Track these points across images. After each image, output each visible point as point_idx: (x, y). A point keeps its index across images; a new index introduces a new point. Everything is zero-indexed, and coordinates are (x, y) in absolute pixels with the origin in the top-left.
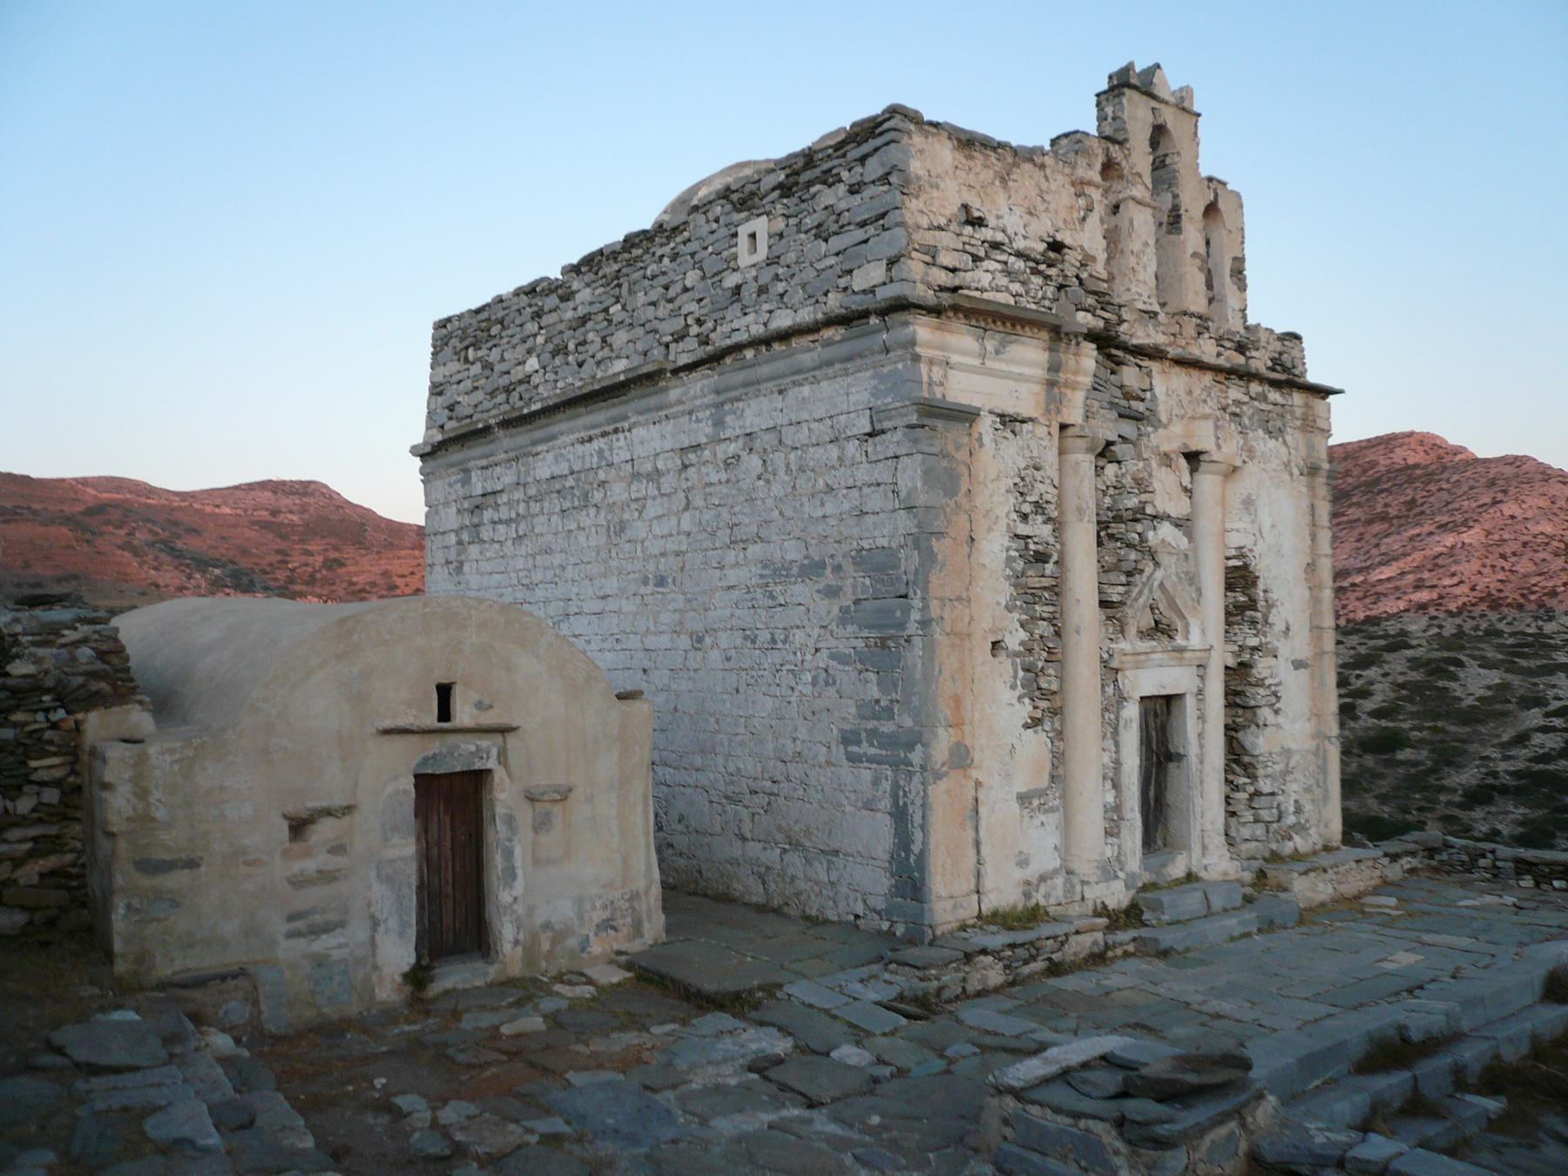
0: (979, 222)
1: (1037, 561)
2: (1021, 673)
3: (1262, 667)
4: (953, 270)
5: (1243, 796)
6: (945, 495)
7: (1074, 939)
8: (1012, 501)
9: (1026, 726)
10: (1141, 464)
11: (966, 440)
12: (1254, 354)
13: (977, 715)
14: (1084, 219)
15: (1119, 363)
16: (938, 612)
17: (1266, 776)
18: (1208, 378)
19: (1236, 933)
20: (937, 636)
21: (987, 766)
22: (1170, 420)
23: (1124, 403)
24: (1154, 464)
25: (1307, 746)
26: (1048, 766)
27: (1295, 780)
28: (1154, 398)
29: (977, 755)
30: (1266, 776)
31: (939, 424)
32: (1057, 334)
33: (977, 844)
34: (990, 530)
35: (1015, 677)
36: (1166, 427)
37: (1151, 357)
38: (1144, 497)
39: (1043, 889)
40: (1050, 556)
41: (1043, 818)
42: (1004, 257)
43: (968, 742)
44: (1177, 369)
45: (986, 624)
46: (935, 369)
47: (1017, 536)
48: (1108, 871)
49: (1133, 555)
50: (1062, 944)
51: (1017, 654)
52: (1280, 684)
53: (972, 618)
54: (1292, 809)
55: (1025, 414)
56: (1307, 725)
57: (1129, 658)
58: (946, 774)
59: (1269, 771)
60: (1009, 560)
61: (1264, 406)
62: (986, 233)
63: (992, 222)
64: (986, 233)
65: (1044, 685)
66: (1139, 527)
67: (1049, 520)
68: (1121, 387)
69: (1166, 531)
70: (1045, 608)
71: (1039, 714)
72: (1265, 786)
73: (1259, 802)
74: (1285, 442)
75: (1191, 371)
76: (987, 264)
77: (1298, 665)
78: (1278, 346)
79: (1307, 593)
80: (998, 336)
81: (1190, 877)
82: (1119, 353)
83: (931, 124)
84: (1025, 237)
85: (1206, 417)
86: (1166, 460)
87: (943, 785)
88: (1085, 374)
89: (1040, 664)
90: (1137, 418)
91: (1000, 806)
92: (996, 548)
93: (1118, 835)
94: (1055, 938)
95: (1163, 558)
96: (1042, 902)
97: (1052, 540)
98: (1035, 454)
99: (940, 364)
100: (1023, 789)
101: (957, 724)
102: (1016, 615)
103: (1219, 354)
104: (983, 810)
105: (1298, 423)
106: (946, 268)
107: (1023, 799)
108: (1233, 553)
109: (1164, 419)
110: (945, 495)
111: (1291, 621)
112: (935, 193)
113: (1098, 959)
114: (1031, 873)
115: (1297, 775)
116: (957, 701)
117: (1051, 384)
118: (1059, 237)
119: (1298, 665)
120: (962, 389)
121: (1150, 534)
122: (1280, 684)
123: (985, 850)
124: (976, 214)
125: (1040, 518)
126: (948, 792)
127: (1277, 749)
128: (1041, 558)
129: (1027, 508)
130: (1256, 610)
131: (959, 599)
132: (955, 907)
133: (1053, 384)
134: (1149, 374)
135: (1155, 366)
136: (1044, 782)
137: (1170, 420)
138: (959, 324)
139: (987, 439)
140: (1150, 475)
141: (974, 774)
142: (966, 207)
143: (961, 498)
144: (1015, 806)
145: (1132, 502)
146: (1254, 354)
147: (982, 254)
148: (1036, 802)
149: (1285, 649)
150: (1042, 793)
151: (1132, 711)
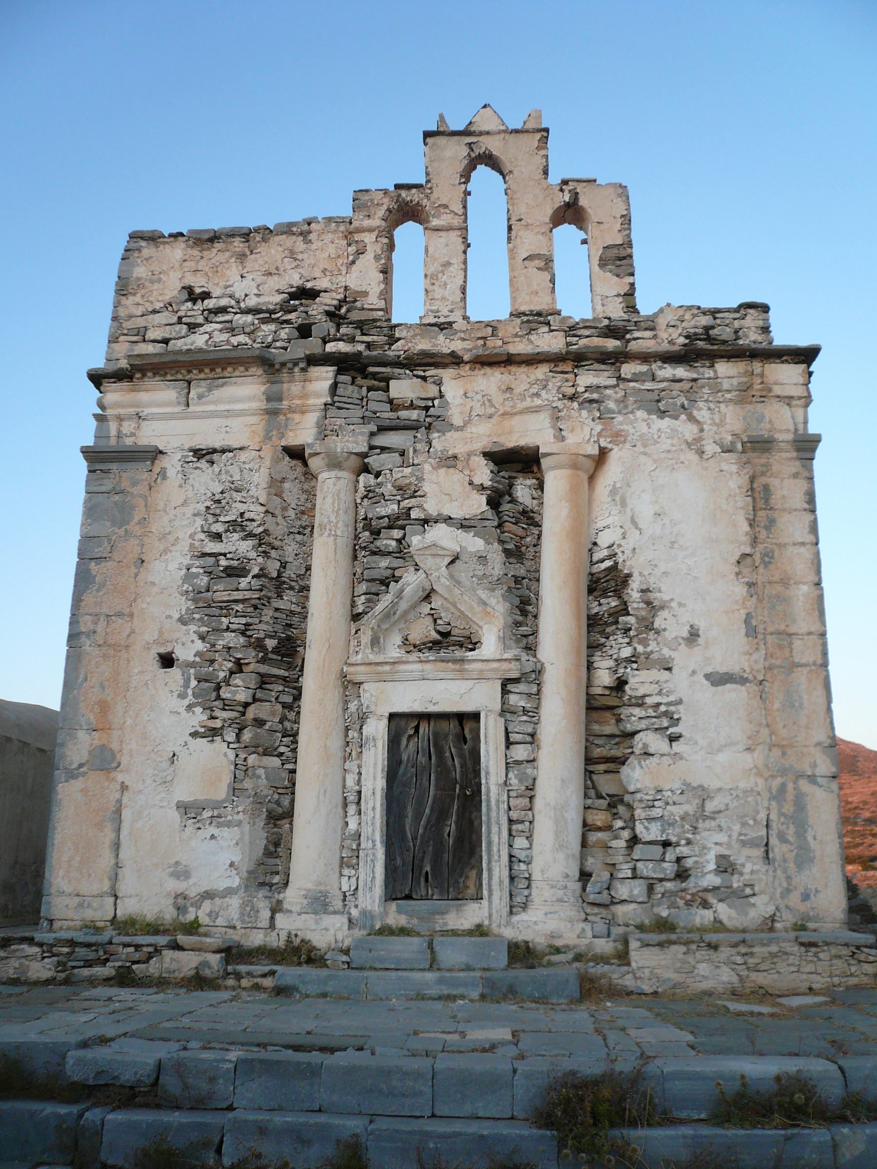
0: (206, 295)
1: (229, 576)
2: (193, 683)
3: (640, 682)
4: (166, 341)
5: (621, 844)
6: (113, 525)
7: (168, 954)
8: (199, 522)
9: (195, 735)
10: (407, 471)
11: (145, 475)
12: (637, 334)
13: (129, 722)
14: (353, 262)
15: (387, 380)
16: (91, 627)
17: (650, 819)
18: (541, 372)
19: (434, 992)
20: (87, 648)
21: (137, 770)
22: (467, 423)
23: (392, 415)
24: (427, 467)
25: (743, 785)
26: (227, 778)
27: (720, 828)
28: (445, 405)
29: (125, 760)
30: (650, 819)
31: (114, 466)
32: (269, 365)
33: (117, 846)
34: (166, 551)
35: (186, 685)
36: (460, 429)
37: (436, 365)
38: (406, 503)
39: (207, 906)
40: (249, 571)
41: (215, 831)
42: (227, 317)
43: (115, 746)
44: (488, 370)
45: (150, 635)
46: (125, 424)
47: (204, 555)
48: (319, 903)
49: (384, 562)
50: (150, 957)
51: (192, 665)
52: (680, 702)
53: (133, 632)
54: (712, 866)
55: (236, 445)
56: (748, 760)
57: (362, 669)
58: (84, 774)
59: (656, 812)
60: (189, 577)
61: (649, 385)
62: (210, 303)
63: (216, 292)
64: (210, 303)
65: (225, 693)
66: (397, 534)
67: (251, 535)
68: (391, 402)
69: (440, 534)
70: (236, 620)
71: (218, 724)
72: (650, 832)
73: (638, 851)
74: (691, 419)
75: (513, 369)
76: (208, 328)
77: (718, 679)
78: (705, 320)
79: (740, 590)
80: (203, 383)
81: (479, 931)
82: (388, 370)
83: (170, 236)
84: (258, 295)
85: (537, 410)
86: (450, 461)
87: (77, 785)
88: (318, 395)
89: (222, 675)
90: (413, 427)
91: (152, 813)
92: (173, 566)
93: (355, 867)
94: (138, 947)
95: (427, 563)
96: (204, 919)
97: (253, 554)
98: (237, 477)
99: (130, 418)
100: (187, 798)
101: (101, 727)
102: (193, 628)
103: (568, 344)
104: (126, 814)
105: (728, 396)
106: (154, 341)
107: (187, 810)
108: (605, 553)
109: (457, 421)
110: (113, 525)
111: (702, 624)
112: (156, 286)
113: (199, 981)
114: (193, 887)
115: (722, 820)
116: (104, 707)
117: (272, 413)
118: (309, 285)
119: (718, 679)
120: (149, 435)
121: (415, 541)
122: (680, 702)
123: (125, 853)
124: (198, 291)
125: (236, 536)
126: (84, 791)
127: (677, 785)
128: (235, 572)
129: (219, 528)
130: (628, 614)
131: (120, 615)
132: (81, 905)
133: (274, 411)
134: (439, 384)
135: (447, 374)
136: (221, 792)
137: (467, 423)
138: (151, 382)
139: (171, 473)
140: (421, 479)
141: (120, 777)
142: (189, 290)
143: (133, 527)
144: (175, 816)
145: (392, 508)
146: (637, 334)
147: (200, 320)
148: (207, 814)
149: (685, 660)
150: (217, 805)
151: (377, 729)
